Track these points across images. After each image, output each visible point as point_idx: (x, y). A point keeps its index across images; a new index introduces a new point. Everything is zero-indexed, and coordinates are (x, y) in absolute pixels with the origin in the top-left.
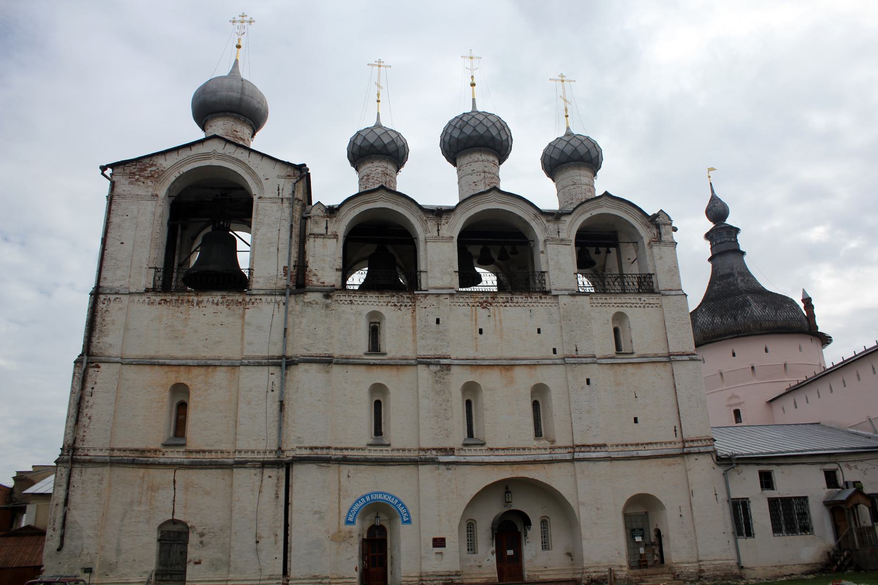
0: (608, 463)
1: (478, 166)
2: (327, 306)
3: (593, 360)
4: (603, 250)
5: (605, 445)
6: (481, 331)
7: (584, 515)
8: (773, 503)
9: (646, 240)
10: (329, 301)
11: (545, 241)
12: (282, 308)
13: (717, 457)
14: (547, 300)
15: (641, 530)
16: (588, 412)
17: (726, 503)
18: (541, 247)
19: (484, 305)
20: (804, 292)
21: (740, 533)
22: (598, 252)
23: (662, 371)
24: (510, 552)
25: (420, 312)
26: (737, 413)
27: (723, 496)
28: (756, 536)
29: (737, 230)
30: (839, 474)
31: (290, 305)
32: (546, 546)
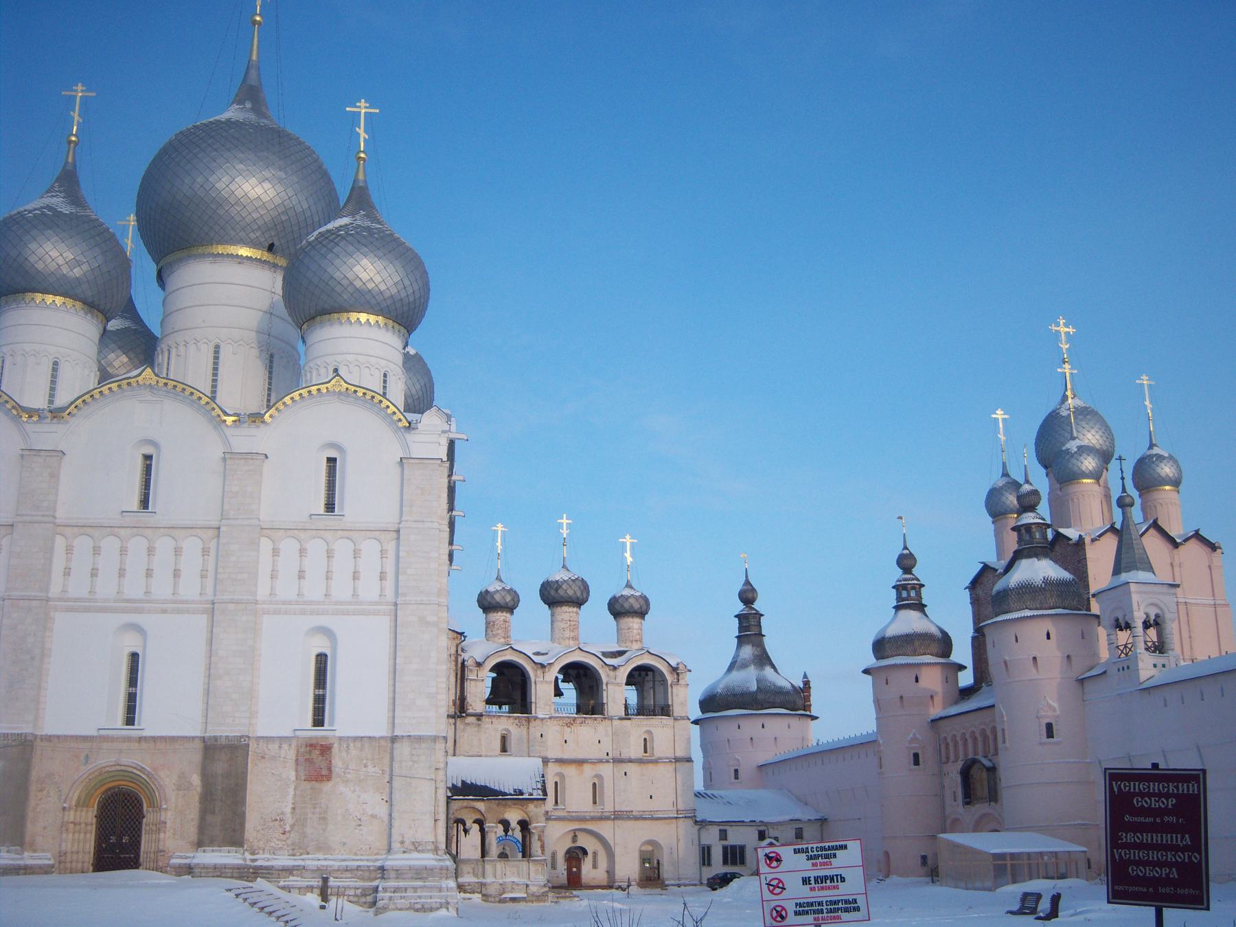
0: (632, 822)
1: (566, 617)
2: (479, 725)
3: (630, 761)
4: (643, 673)
5: (632, 811)
6: (566, 742)
7: (618, 851)
8: (725, 848)
9: (669, 683)
10: (480, 722)
11: (607, 684)
12: (453, 727)
13: (696, 820)
14: (607, 722)
15: (649, 859)
16: (624, 791)
17: (698, 848)
18: (604, 687)
19: (569, 725)
20: (805, 676)
21: (704, 864)
22: (640, 675)
23: (670, 768)
24: (574, 870)
25: (532, 730)
26: (736, 771)
27: (696, 842)
28: (713, 866)
29: (762, 615)
30: (766, 832)
31: (457, 725)
32: (595, 866)
